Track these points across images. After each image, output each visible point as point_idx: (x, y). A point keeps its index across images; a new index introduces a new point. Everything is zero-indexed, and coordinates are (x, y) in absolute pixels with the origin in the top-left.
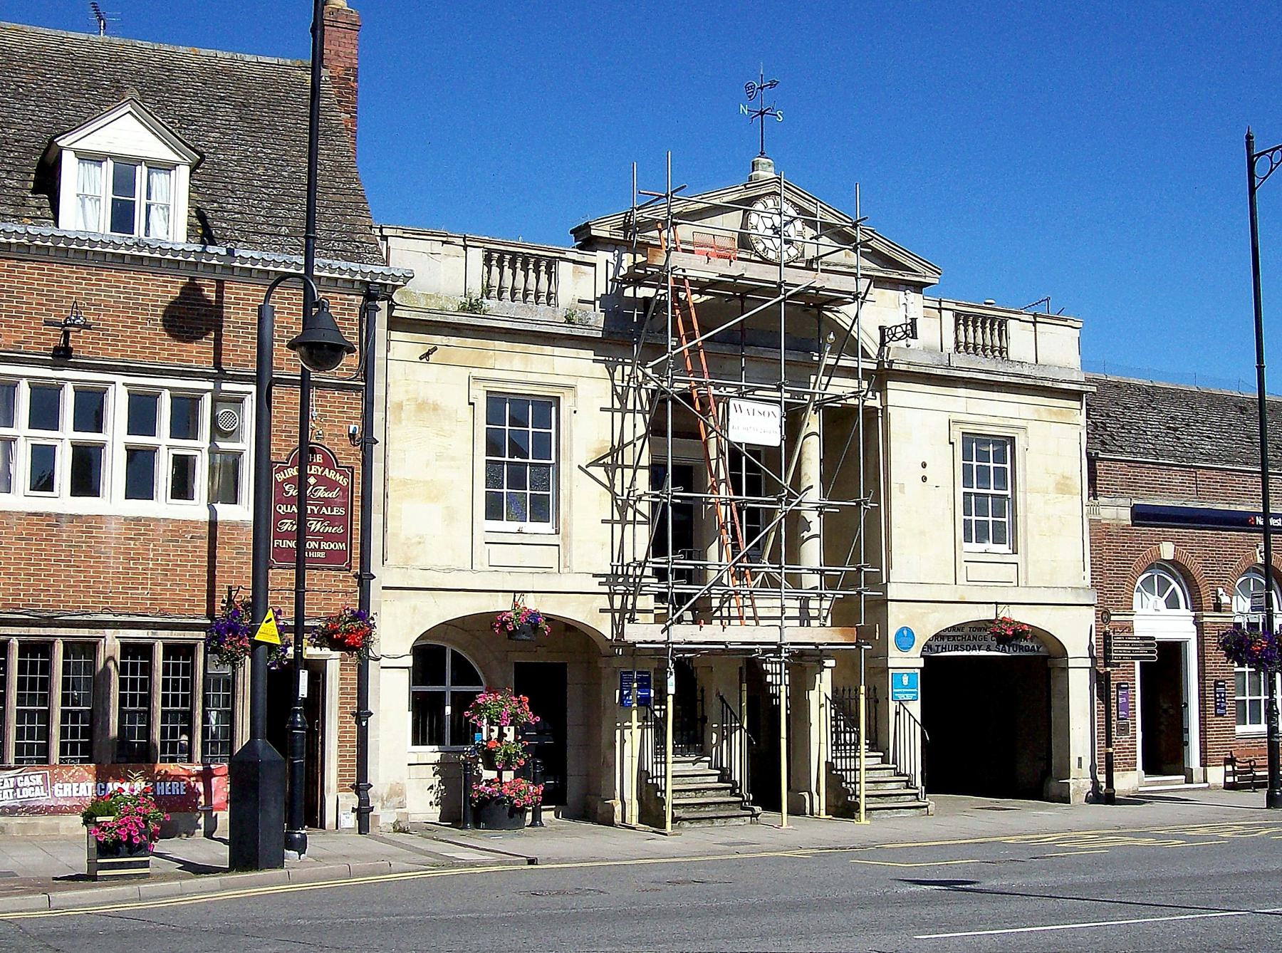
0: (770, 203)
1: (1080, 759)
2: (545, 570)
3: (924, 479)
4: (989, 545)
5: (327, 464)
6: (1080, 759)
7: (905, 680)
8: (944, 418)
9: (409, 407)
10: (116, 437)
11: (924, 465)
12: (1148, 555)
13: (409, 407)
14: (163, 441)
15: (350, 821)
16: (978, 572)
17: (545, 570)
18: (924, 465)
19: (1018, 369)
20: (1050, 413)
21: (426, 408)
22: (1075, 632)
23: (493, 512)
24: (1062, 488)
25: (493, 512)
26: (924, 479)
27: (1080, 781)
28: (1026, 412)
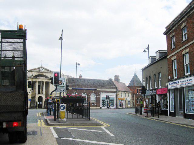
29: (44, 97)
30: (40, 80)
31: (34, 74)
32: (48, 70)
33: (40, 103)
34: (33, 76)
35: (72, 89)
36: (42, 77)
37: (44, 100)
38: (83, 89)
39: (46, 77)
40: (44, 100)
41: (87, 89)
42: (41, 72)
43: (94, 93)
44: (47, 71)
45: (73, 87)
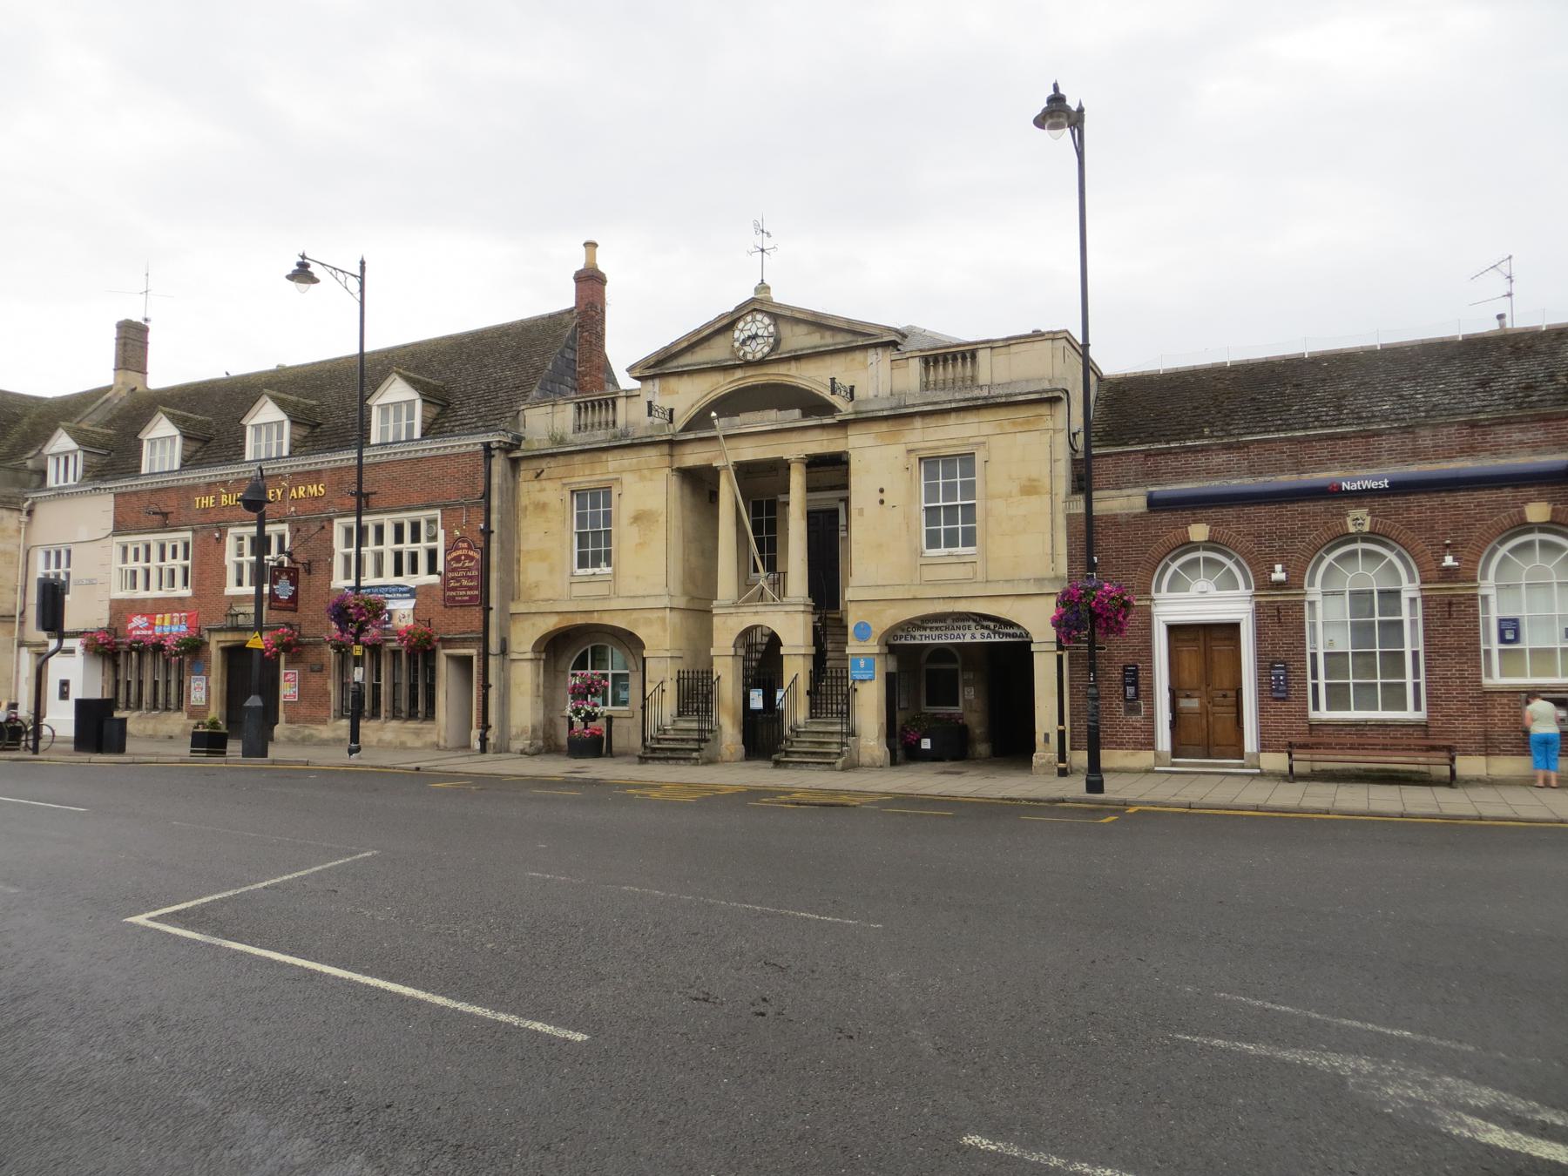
0: (749, 318)
1: (1047, 736)
2: (605, 598)
3: (882, 502)
4: (960, 550)
5: (470, 548)
6: (1047, 736)
7: (862, 663)
8: (901, 449)
9: (530, 508)
10: (389, 545)
11: (882, 491)
12: (1173, 537)
13: (530, 508)
14: (407, 546)
15: (477, 745)
16: (929, 574)
17: (605, 598)
18: (882, 491)
19: (976, 393)
20: (1014, 424)
21: (542, 507)
22: (1037, 621)
23: (582, 563)
24: (1030, 489)
25: (582, 563)
26: (882, 502)
27: (1044, 753)
28: (987, 429)
29: (793, 630)
30: (750, 452)
31: (686, 396)
32: (818, 323)
33: (769, 699)
34: (679, 423)
35: (1154, 504)
36: (770, 418)
37: (796, 669)
38: (1331, 493)
39: (813, 405)
40: (796, 669)
41: (1399, 488)
42: (748, 364)
43: (1212, 544)
44: (813, 340)
45: (1152, 475)
